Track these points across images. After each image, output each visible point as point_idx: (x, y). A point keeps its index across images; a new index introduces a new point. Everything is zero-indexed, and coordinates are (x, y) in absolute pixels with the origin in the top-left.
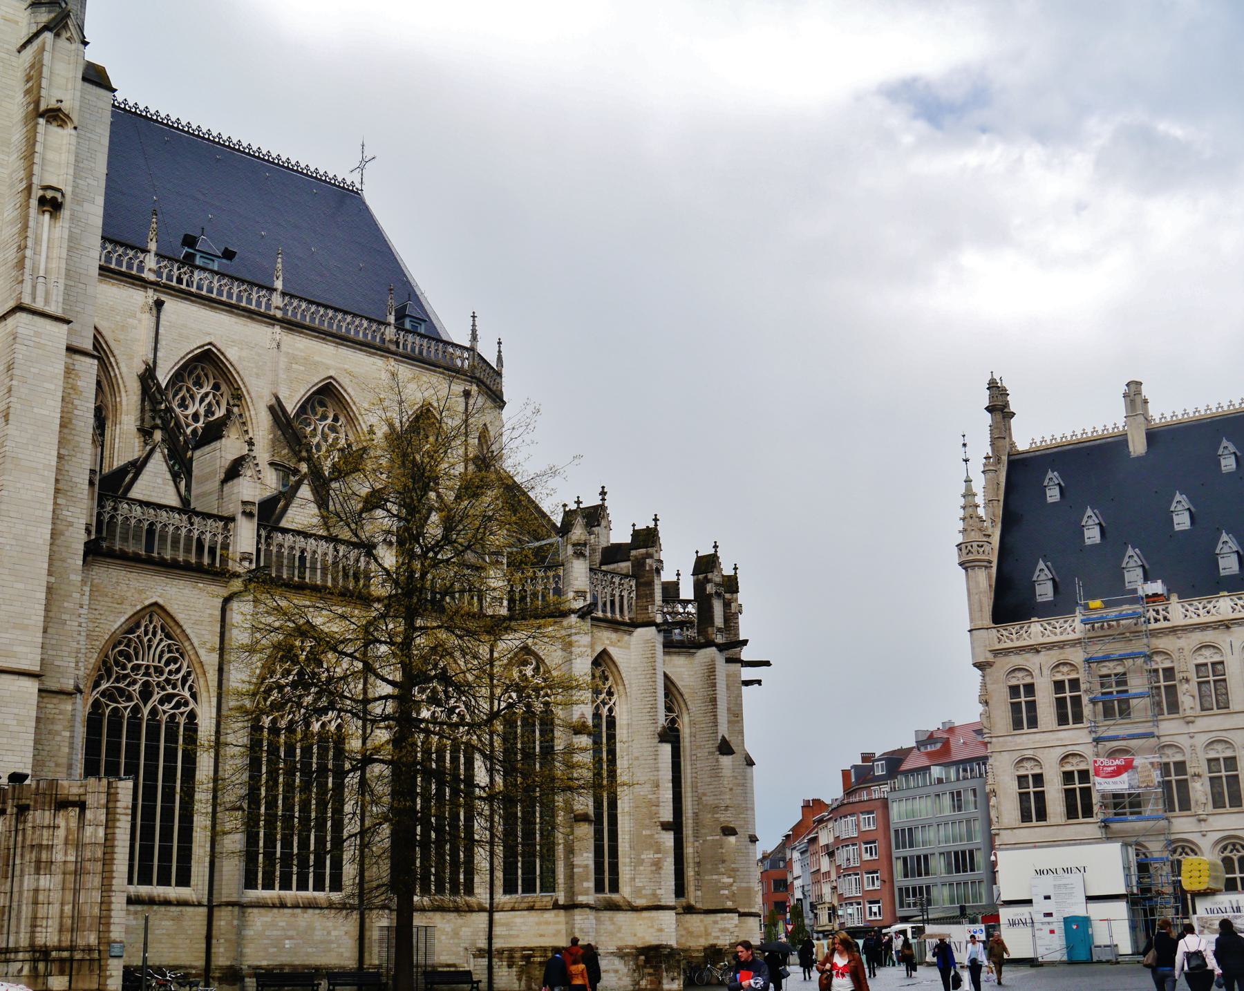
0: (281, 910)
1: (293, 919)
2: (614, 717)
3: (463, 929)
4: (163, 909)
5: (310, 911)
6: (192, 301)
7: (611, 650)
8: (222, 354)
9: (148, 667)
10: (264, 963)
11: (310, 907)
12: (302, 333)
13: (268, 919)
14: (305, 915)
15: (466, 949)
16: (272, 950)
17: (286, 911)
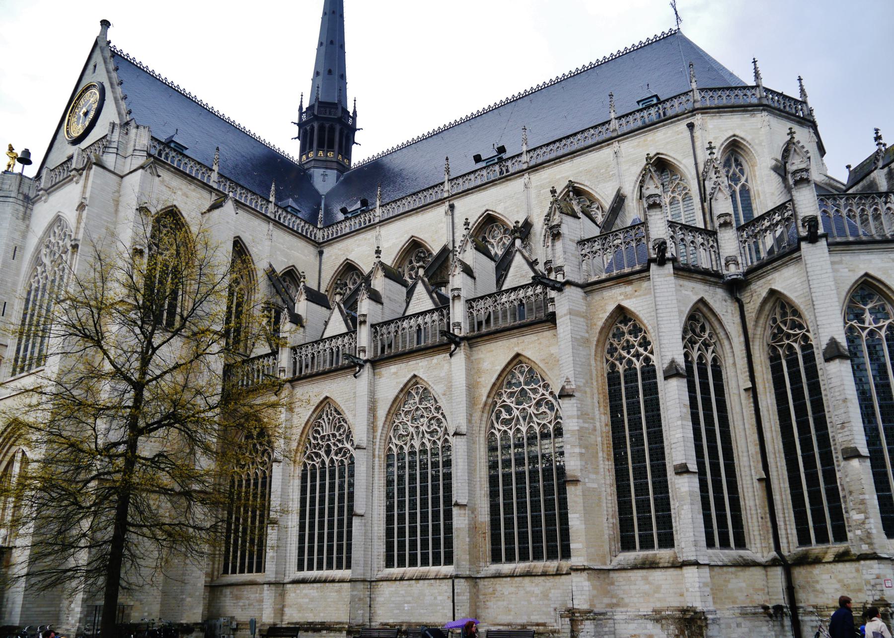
0: (401, 582)
1: (409, 588)
2: (653, 365)
3: (553, 591)
4: (331, 585)
5: (421, 582)
6: (472, 193)
7: (626, 304)
8: (495, 212)
9: (329, 435)
10: (391, 621)
11: (420, 579)
12: (544, 167)
13: (393, 589)
14: (418, 585)
15: (555, 610)
16: (396, 611)
17: (405, 582)
